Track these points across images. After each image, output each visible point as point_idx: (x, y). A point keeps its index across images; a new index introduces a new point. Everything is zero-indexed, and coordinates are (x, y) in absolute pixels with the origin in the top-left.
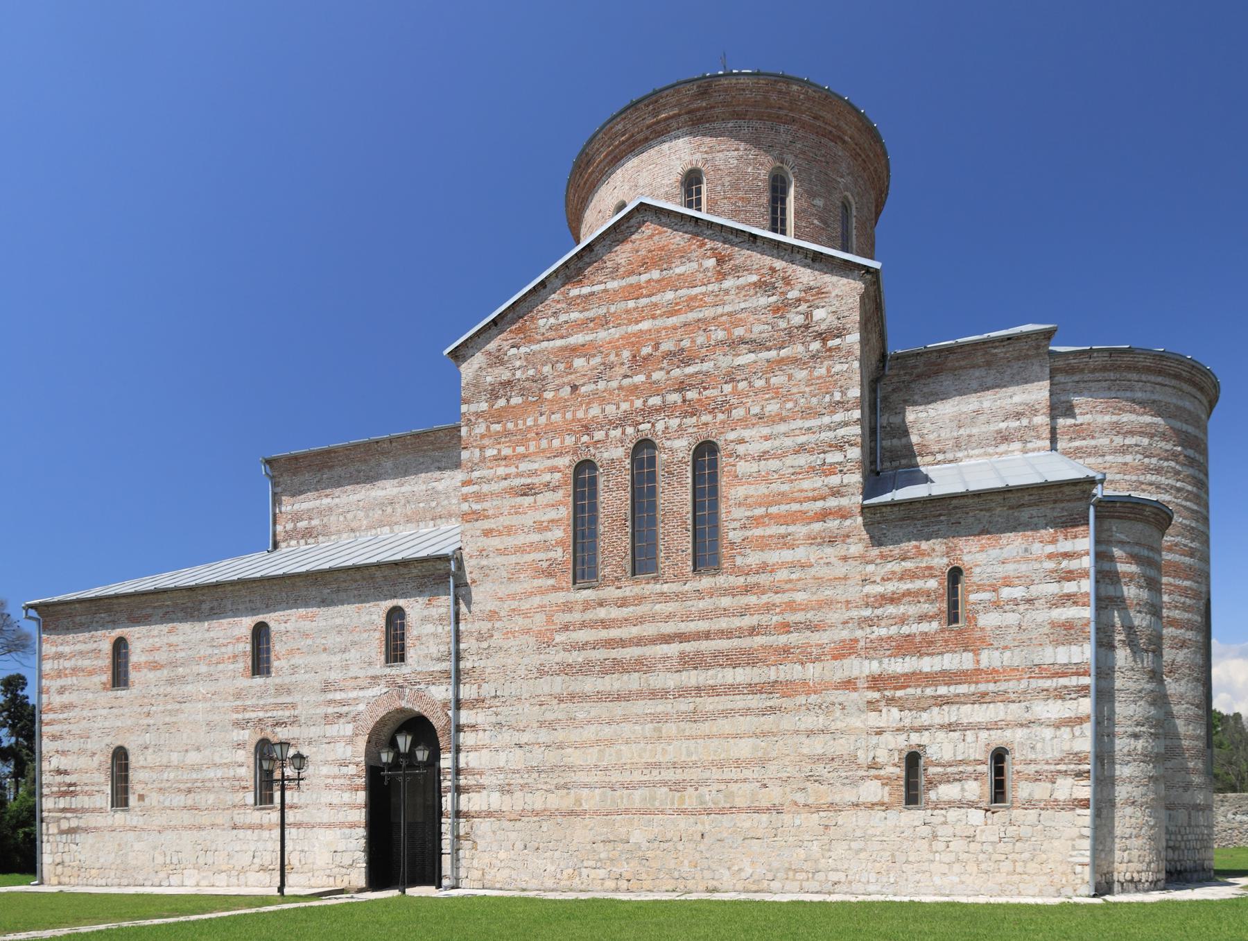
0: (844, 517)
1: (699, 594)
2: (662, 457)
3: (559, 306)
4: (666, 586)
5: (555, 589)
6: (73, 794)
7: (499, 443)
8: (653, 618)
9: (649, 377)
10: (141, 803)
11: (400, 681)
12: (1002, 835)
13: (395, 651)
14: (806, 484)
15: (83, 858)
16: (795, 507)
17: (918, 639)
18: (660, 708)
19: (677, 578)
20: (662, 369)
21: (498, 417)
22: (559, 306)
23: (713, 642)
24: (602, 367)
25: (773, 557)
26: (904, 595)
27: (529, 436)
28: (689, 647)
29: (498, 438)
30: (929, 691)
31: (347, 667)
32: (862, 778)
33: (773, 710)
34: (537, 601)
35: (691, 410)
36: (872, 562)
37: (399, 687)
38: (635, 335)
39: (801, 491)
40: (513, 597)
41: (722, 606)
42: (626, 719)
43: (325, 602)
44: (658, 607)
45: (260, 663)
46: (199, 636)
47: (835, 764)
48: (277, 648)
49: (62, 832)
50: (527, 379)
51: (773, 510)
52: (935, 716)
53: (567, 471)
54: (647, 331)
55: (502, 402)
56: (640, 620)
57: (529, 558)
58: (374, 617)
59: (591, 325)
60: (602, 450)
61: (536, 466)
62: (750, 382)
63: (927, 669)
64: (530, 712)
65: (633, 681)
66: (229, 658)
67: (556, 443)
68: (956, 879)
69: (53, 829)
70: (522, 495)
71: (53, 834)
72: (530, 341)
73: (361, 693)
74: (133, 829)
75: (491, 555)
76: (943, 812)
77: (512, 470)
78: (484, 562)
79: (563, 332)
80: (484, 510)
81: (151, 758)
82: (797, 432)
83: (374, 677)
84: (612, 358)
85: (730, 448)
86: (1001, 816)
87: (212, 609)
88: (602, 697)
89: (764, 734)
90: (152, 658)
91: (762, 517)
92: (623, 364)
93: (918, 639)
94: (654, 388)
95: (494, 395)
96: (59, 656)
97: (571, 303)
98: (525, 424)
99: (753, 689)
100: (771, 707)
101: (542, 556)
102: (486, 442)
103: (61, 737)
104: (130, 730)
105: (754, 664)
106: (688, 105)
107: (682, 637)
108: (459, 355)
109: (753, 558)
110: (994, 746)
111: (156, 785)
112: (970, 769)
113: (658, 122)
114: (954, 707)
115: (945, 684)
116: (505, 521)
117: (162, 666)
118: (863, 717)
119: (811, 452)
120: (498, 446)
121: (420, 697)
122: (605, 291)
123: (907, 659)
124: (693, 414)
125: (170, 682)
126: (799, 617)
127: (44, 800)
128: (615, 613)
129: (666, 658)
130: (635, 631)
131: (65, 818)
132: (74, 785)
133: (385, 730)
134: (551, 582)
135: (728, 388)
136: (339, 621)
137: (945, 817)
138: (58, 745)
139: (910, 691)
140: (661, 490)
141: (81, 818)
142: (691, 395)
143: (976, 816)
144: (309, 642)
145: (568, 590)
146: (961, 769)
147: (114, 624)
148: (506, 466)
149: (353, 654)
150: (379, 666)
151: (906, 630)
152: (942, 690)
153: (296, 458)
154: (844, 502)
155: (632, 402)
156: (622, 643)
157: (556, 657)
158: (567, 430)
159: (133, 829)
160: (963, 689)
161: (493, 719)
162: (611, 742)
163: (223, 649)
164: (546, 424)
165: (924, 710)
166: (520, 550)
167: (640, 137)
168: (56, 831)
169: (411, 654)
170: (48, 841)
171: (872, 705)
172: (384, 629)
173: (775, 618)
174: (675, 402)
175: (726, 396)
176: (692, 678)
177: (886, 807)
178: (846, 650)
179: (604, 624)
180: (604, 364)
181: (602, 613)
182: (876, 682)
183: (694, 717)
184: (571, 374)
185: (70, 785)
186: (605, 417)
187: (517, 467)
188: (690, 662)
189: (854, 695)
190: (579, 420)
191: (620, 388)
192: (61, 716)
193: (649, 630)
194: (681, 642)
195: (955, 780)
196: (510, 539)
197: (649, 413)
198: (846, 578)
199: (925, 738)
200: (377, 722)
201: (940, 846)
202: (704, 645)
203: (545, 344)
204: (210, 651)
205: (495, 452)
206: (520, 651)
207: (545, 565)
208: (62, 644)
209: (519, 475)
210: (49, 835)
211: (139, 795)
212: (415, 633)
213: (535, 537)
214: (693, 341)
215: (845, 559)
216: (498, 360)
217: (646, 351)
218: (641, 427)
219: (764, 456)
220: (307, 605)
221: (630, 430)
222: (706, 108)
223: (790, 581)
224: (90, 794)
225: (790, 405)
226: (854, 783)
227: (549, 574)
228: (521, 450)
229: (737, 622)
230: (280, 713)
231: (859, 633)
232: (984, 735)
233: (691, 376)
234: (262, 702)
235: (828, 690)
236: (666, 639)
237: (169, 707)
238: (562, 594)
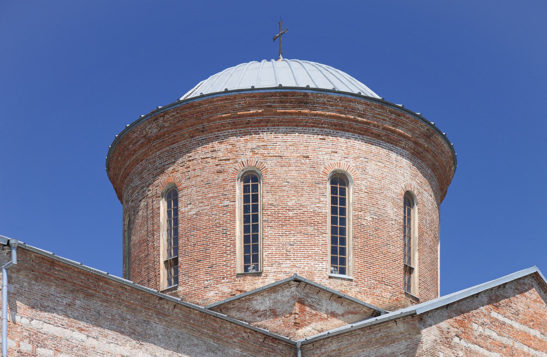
106: (417, 137)
113: (393, 132)
153: (53, 262)
167: (375, 130)
222: (424, 149)
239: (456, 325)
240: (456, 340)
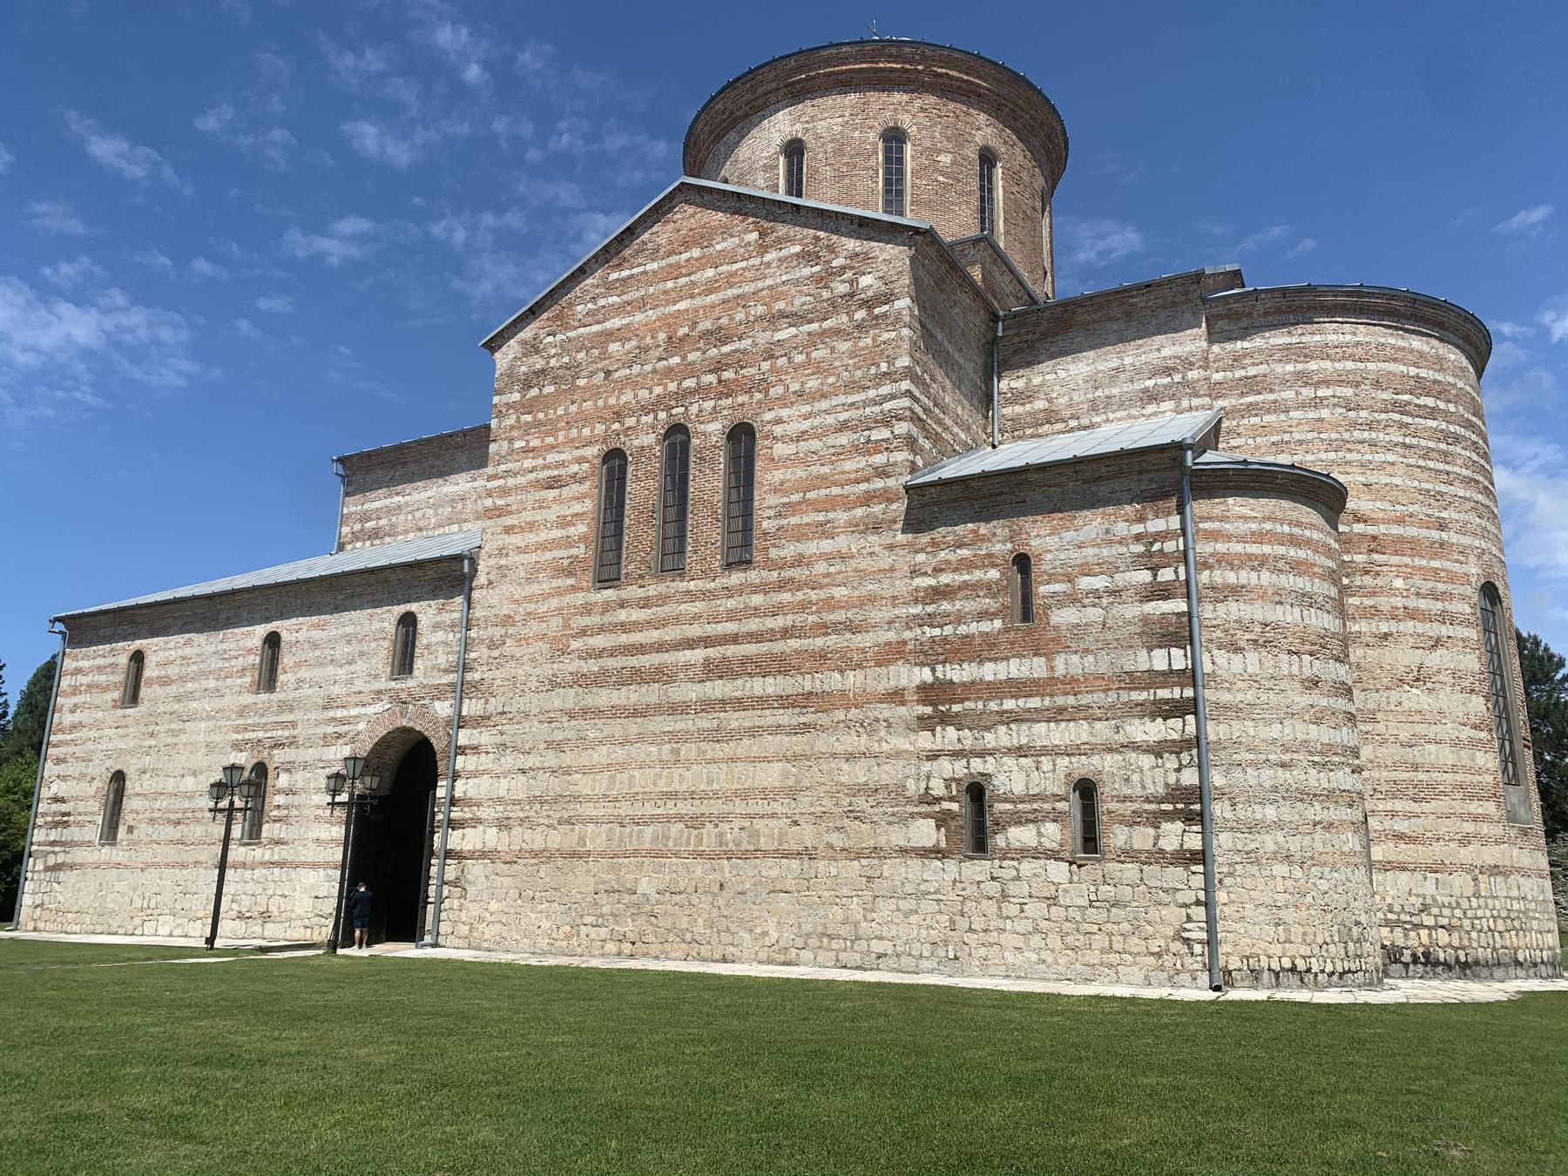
0: (890, 501)
1: (729, 592)
2: (695, 442)
3: (597, 291)
4: (692, 583)
5: (574, 589)
6: (66, 824)
7: (528, 434)
8: (677, 620)
9: (684, 358)
10: (130, 837)
11: (403, 696)
12: (1093, 897)
13: (404, 661)
14: (849, 466)
15: (62, 900)
16: (836, 491)
17: (978, 640)
18: (681, 725)
19: (706, 574)
20: (698, 349)
21: (528, 407)
22: (597, 291)
24: (637, 351)
25: (812, 547)
26: (960, 588)
27: (559, 426)
28: (713, 652)
29: (526, 429)
30: (993, 706)
31: (351, 682)
32: (912, 816)
33: (805, 728)
34: (554, 603)
35: (725, 389)
36: (922, 550)
37: (402, 703)
38: (671, 315)
39: (843, 473)
40: (529, 599)
41: (753, 604)
42: (641, 738)
43: (337, 609)
44: (683, 607)
45: (268, 677)
46: (212, 648)
47: (880, 796)
48: (285, 660)
49: (48, 869)
50: (561, 367)
51: (811, 495)
52: (1001, 737)
53: (595, 461)
54: (684, 311)
55: (534, 392)
56: (662, 623)
57: (548, 556)
58: (386, 624)
59: (629, 308)
60: (632, 437)
61: (563, 457)
62: (789, 358)
63: (989, 678)
64: (537, 728)
65: (651, 694)
66: (237, 672)
67: (586, 432)
68: (1034, 957)
69: (40, 866)
70: (547, 488)
71: (38, 871)
73: (363, 711)
74: (117, 866)
75: (511, 553)
76: (1015, 863)
77: (540, 462)
78: (503, 562)
79: (600, 317)
80: (508, 505)
81: (149, 784)
82: (839, 409)
83: (379, 692)
84: (648, 340)
85: (766, 429)
86: (1092, 871)
87: (228, 618)
88: (616, 712)
89: (795, 758)
90: (164, 673)
91: (799, 503)
92: (658, 346)
93: (978, 640)
94: (689, 370)
95: (527, 385)
96: (78, 671)
97: (610, 288)
98: (555, 413)
99: (785, 702)
100: (804, 724)
101: (564, 553)
102: (515, 433)
103: (64, 761)
104: (131, 752)
105: (786, 673)
107: (707, 642)
108: (493, 345)
109: (790, 550)
110: (1077, 777)
111: (147, 815)
112: (1047, 806)
114: (1024, 727)
115: (1012, 697)
116: (528, 516)
117: (173, 681)
118: (913, 736)
119: (854, 429)
120: (526, 438)
121: (424, 712)
122: (645, 273)
123: (965, 665)
124: (728, 396)
125: (178, 699)
126: (840, 616)
127: (36, 831)
128: (637, 615)
129: (688, 666)
130: (654, 635)
131: (53, 852)
132: (68, 814)
133: (391, 751)
135: (766, 366)
136: (350, 629)
137: (1017, 870)
138: (61, 769)
139: (969, 705)
140: (691, 477)
141: (68, 853)
143: (1058, 871)
144: (318, 653)
145: (588, 591)
146: (1035, 806)
147: (135, 636)
148: (533, 458)
149: (361, 666)
150: (383, 680)
151: (963, 629)
152: (1009, 704)
154: (891, 482)
155: (666, 385)
156: (642, 649)
157: (573, 665)
158: (598, 417)
159: (117, 866)
160: (1034, 702)
161: (498, 739)
162: (622, 767)
163: (233, 662)
164: (578, 413)
165: (988, 729)
166: (542, 547)
168: (42, 868)
169: (419, 665)
170: (32, 880)
171: (926, 723)
172: (393, 638)
173: (811, 618)
174: (711, 383)
175: (764, 374)
176: (720, 688)
177: (937, 853)
179: (625, 627)
180: (639, 347)
181: (622, 615)
183: (718, 735)
184: (605, 359)
185: (64, 814)
186: (638, 402)
187: (544, 459)
188: (713, 671)
189: (902, 710)
190: (610, 407)
191: (654, 371)
192: (68, 737)
193: (671, 634)
194: (706, 648)
195: (1028, 821)
196: (531, 535)
197: (682, 396)
198: (892, 569)
199: (989, 765)
200: (377, 744)
201: (1012, 910)
202: (731, 650)
203: (582, 330)
204: (220, 664)
205: (523, 444)
206: (533, 660)
207: (566, 562)
208: (82, 659)
209: (545, 467)
210: (33, 872)
211: (129, 826)
212: (425, 641)
213: (557, 533)
214: (731, 318)
215: (891, 547)
216: (533, 348)
217: (682, 331)
218: (674, 411)
219: (802, 436)
220: (320, 614)
221: (662, 415)
223: (829, 575)
224: (80, 825)
225: (832, 380)
226: (904, 820)
227: (571, 574)
228: (549, 440)
229: (771, 623)
230: (280, 733)
231: (908, 635)
232: (1063, 762)
233: (728, 355)
234: (263, 721)
235: (871, 703)
236: (690, 644)
237: (173, 726)
238: (580, 595)
239: (550, 323)
240: (551, 339)
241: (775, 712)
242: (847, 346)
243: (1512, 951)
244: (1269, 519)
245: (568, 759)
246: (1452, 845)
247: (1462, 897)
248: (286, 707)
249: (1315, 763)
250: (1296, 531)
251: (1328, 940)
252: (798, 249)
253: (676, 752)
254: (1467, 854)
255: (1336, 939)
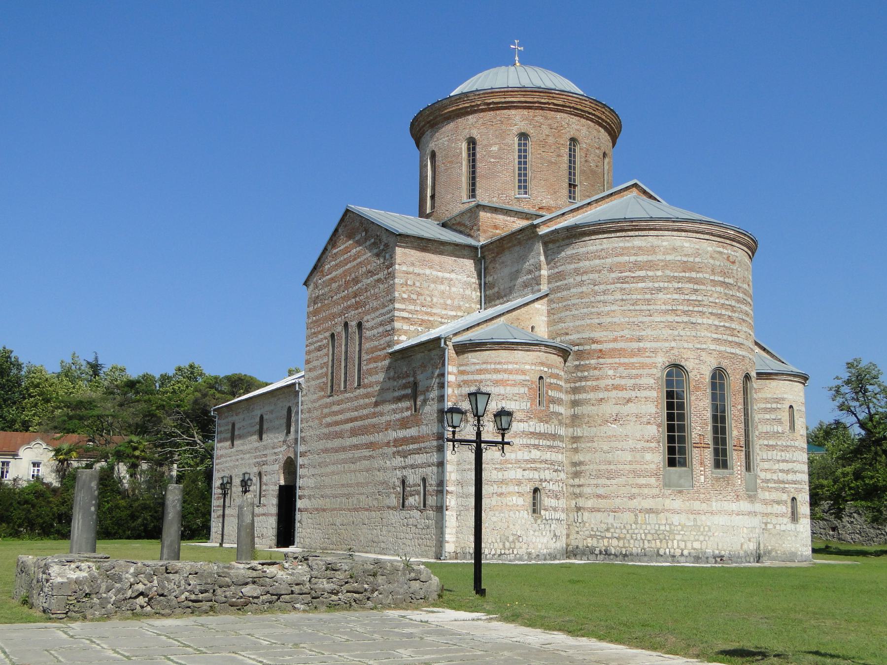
1: (357, 398)
5: (324, 397)
14: (382, 342)
23: (358, 422)
35: (357, 306)
52: (410, 460)
65: (337, 443)
72: (324, 276)
107: (352, 420)
134: (323, 393)
142: (357, 299)
152: (411, 447)
160: (416, 446)
176: (355, 440)
178: (388, 426)
182: (398, 442)
188: (354, 433)
240: (320, 281)
241: (365, 450)
242: (381, 286)
243: (656, 550)
244: (484, 363)
245: (323, 470)
246: (625, 499)
247: (627, 524)
248: (265, 447)
249: (496, 468)
250: (498, 367)
251: (494, 541)
252: (373, 240)
253: (344, 467)
254: (634, 503)
255: (499, 541)
